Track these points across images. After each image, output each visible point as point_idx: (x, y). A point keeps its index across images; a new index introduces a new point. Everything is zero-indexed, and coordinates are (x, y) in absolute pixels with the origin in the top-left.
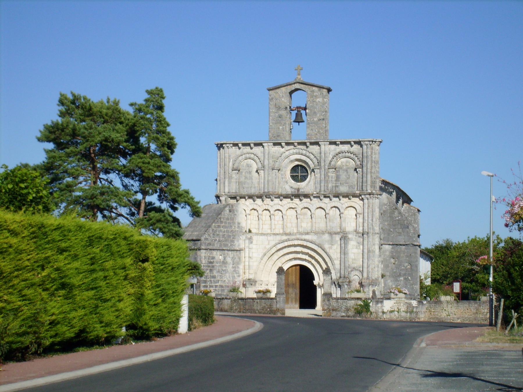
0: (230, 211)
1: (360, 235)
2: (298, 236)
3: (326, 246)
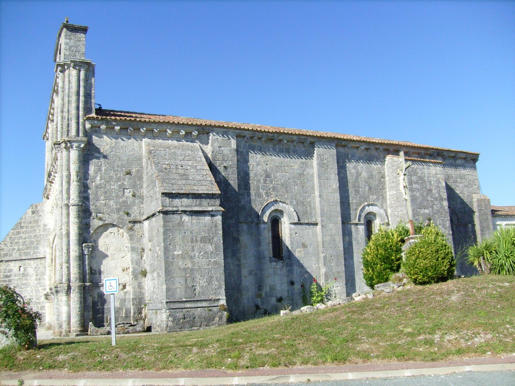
0: (33, 213)
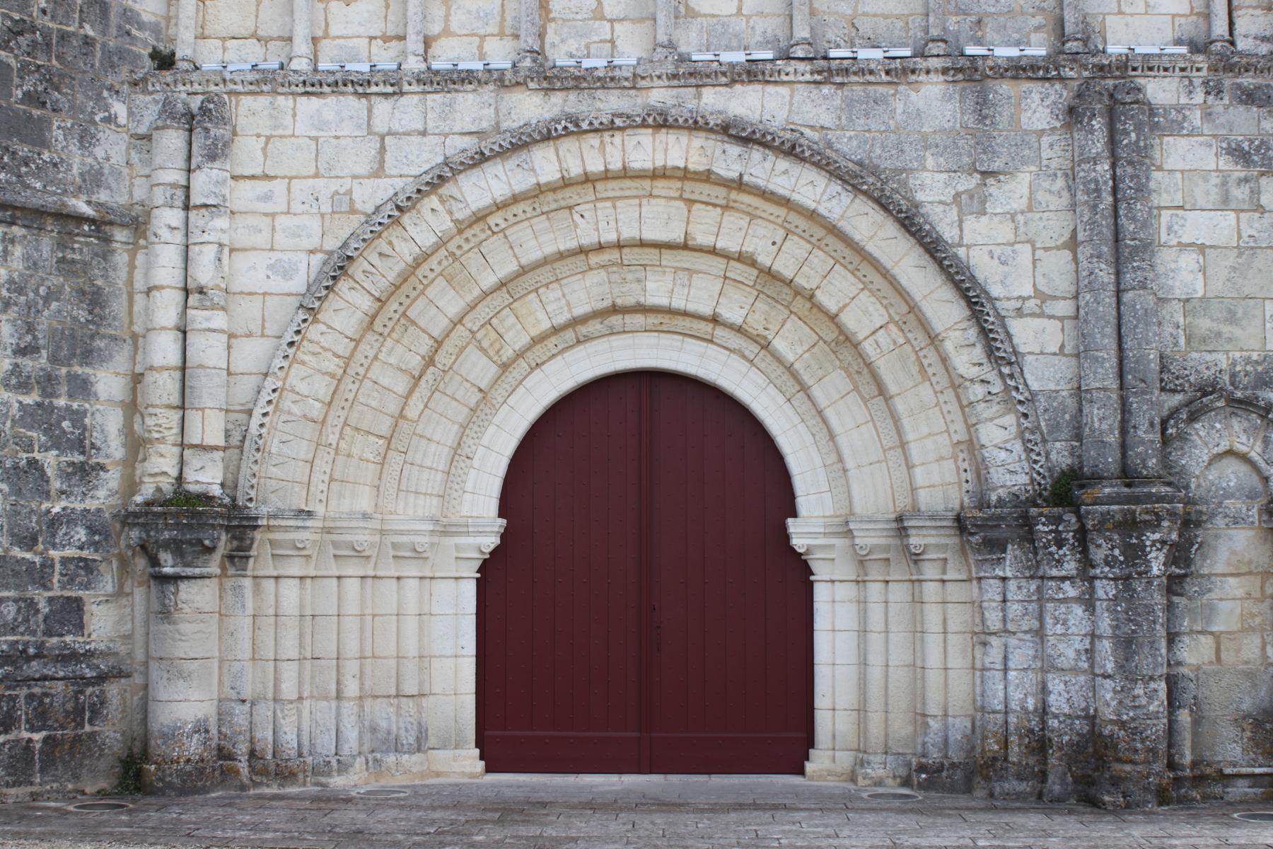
1: (1247, 80)
2: (659, 96)
3: (932, 189)
